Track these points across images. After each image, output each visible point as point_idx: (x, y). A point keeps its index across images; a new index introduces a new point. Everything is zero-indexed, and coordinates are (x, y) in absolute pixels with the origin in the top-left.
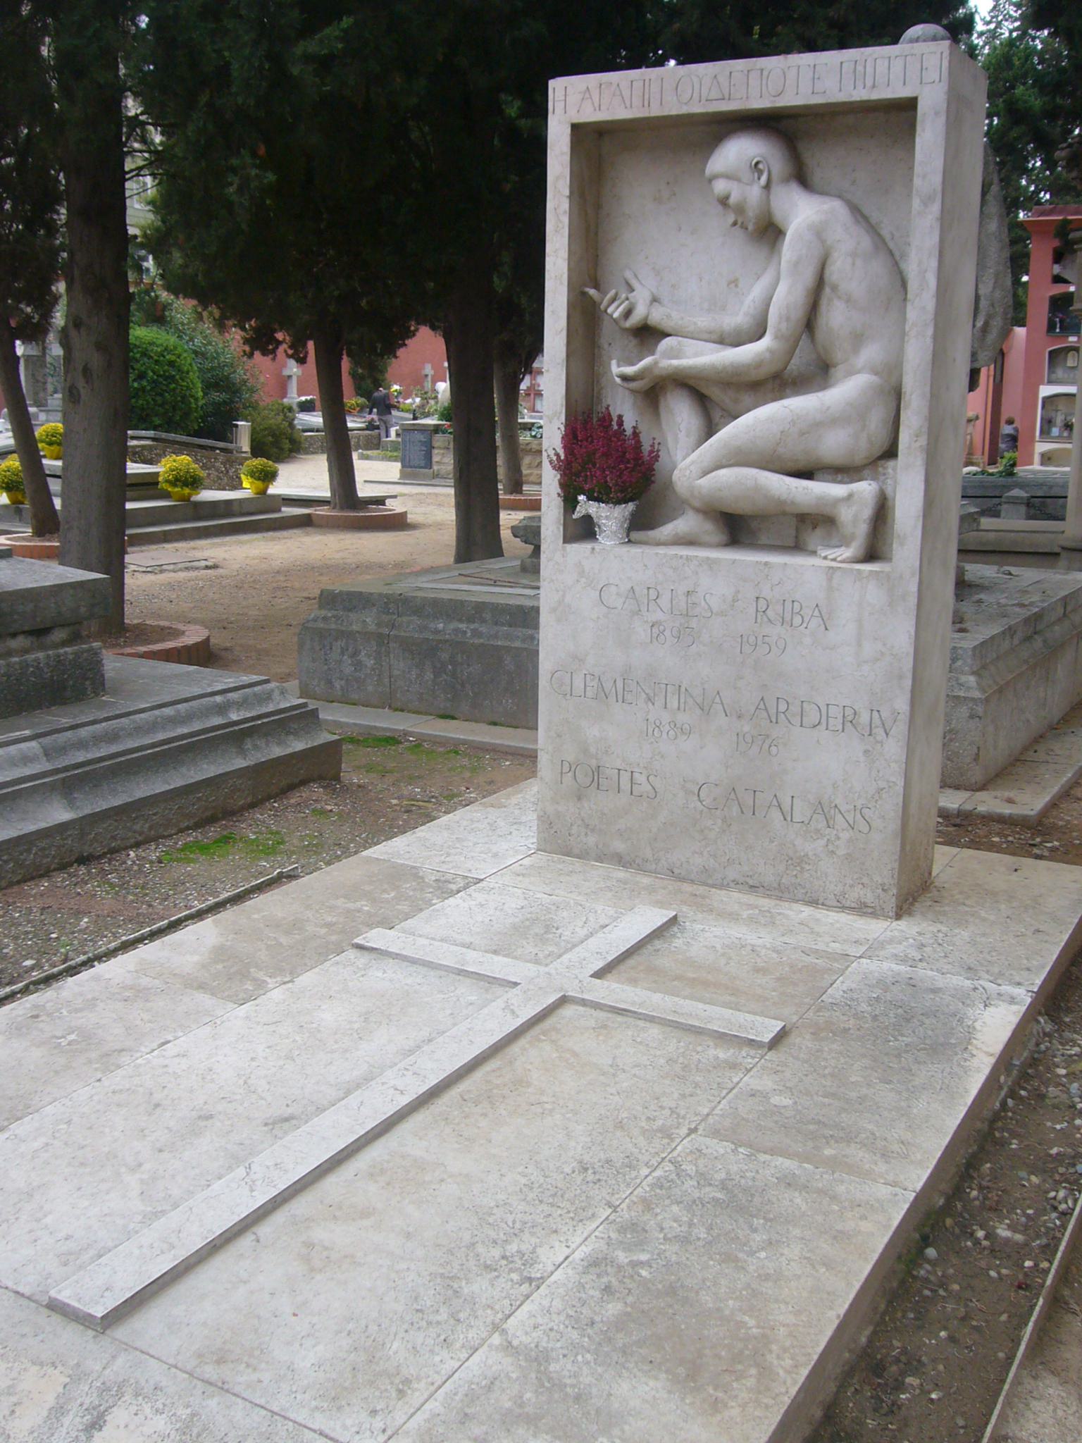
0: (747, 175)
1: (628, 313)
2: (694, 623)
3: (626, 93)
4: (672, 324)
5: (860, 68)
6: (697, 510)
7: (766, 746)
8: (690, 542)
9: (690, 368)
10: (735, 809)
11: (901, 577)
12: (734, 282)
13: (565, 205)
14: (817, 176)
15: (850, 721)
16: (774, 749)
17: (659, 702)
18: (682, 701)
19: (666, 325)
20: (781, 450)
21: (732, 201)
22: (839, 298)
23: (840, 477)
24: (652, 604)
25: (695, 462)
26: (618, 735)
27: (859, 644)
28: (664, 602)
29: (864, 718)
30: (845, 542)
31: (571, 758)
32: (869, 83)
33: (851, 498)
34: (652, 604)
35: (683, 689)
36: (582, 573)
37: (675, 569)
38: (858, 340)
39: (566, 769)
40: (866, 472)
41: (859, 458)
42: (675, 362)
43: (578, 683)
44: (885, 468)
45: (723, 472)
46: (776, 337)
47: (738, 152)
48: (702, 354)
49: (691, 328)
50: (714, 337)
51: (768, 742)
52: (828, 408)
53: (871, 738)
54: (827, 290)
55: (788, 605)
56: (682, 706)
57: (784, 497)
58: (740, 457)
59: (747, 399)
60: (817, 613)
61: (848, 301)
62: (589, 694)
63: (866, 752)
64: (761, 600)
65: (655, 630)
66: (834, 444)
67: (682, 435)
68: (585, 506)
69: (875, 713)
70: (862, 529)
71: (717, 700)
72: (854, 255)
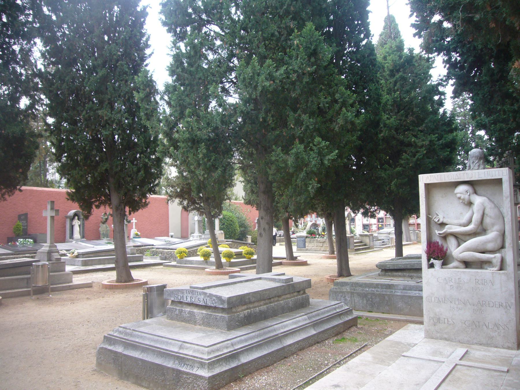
0: (465, 193)
1: (438, 221)
2: (461, 285)
6: (458, 261)
8: (457, 268)
10: (474, 327)
12: (462, 213)
13: (424, 199)
14: (479, 192)
15: (501, 305)
17: (453, 302)
19: (447, 222)
25: (457, 251)
28: (453, 281)
29: (504, 304)
31: (432, 316)
33: (496, 257)
38: (493, 225)
41: (496, 249)
42: (451, 230)
43: (433, 299)
46: (475, 225)
47: (462, 188)
54: (485, 215)
59: (468, 237)
66: (490, 246)
68: (432, 261)
70: (499, 264)
72: (491, 208)
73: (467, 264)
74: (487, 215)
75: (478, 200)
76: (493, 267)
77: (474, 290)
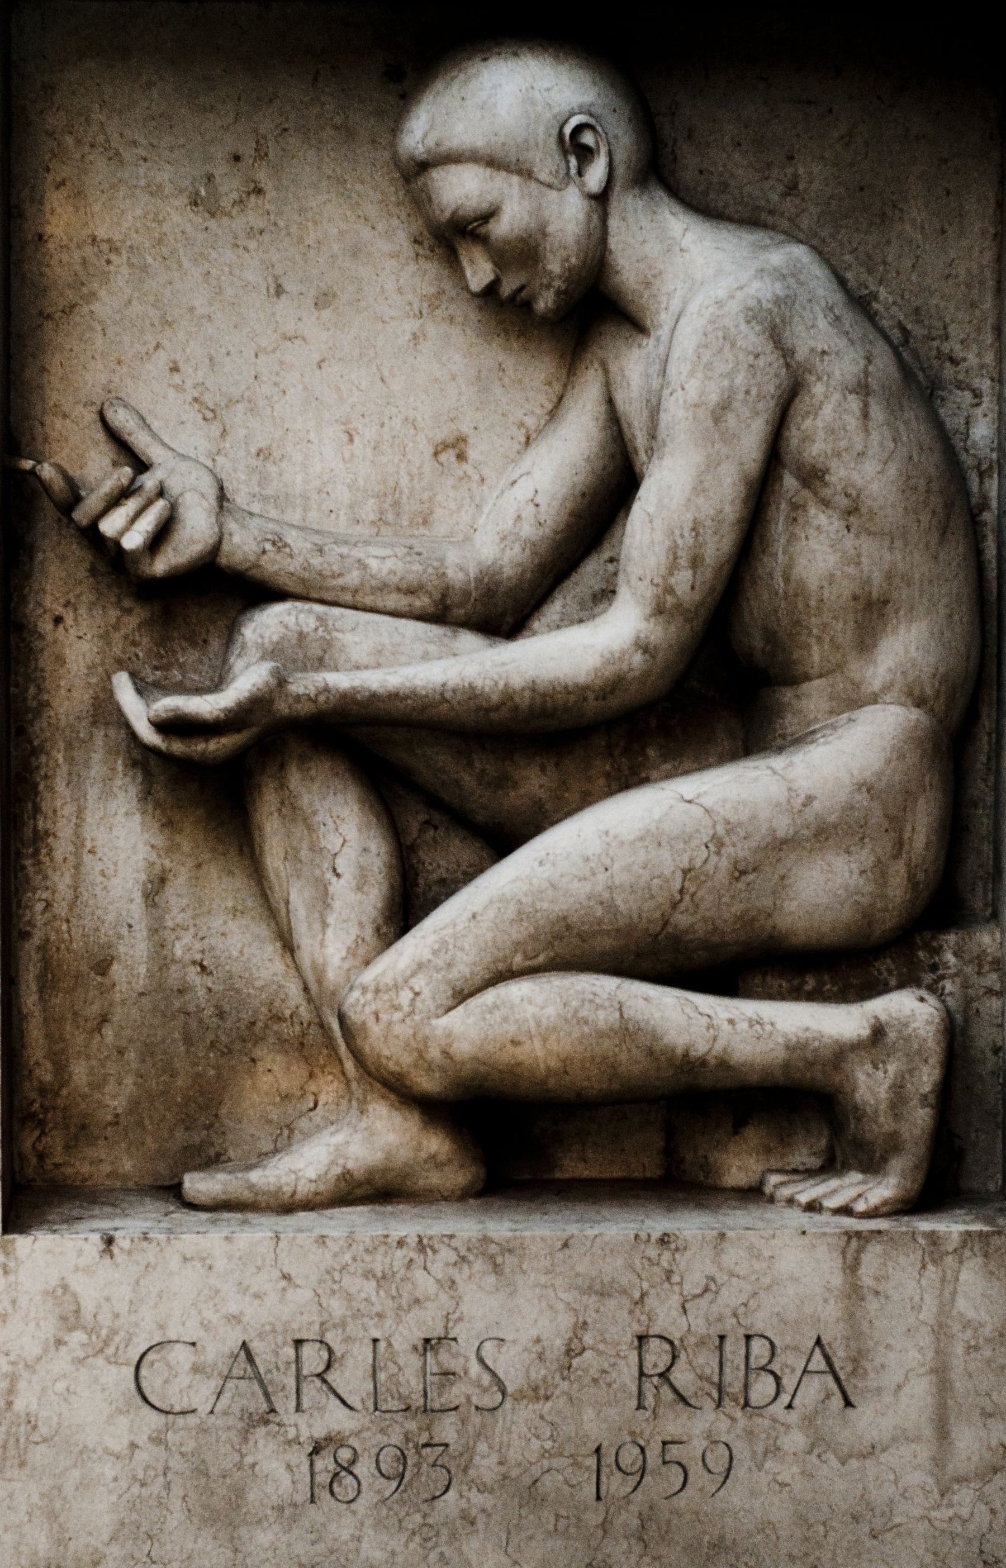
0: (547, 163)
1: (161, 535)
2: (447, 1430)
4: (294, 566)
9: (394, 696)
12: (456, 447)
14: (689, 164)
19: (275, 566)
20: (682, 920)
21: (502, 228)
22: (826, 503)
24: (312, 1390)
28: (352, 1379)
30: (872, 1165)
34: (312, 1390)
36: (72, 1319)
37: (383, 1279)
38: (872, 613)
40: (885, 966)
42: (341, 681)
44: (938, 951)
45: (517, 990)
49: (353, 578)
50: (421, 602)
52: (809, 799)
55: (734, 1349)
59: (534, 781)
60: (818, 1362)
64: (654, 1344)
65: (325, 1463)
66: (823, 893)
67: (341, 889)
72: (862, 389)
73: (511, 1138)
74: (813, 477)
76: (830, 1166)
77: (615, 1485)
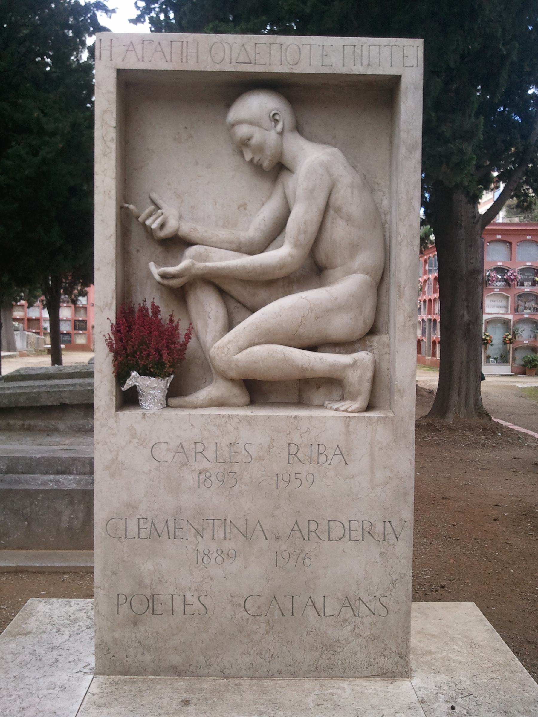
1: (162, 226)
2: (236, 468)
3: (167, 50)
4: (198, 235)
5: (358, 51)
6: (232, 380)
7: (301, 559)
8: (221, 404)
9: (224, 269)
10: (277, 613)
11: (402, 420)
12: (244, 206)
13: (113, 134)
15: (368, 532)
16: (307, 561)
17: (207, 535)
18: (228, 531)
19: (194, 235)
20: (301, 330)
21: (254, 141)
22: (341, 218)
23: (337, 350)
24: (199, 456)
25: (230, 343)
26: (171, 568)
27: (372, 473)
28: (210, 453)
29: (379, 528)
30: (353, 398)
31: (127, 590)
32: (365, 62)
33: (355, 364)
34: (199, 456)
35: (228, 522)
36: (134, 435)
37: (218, 426)
38: (354, 248)
39: (122, 599)
40: (358, 345)
41: (358, 334)
42: (209, 264)
43: (132, 526)
44: (372, 342)
45: (256, 348)
46: (296, 245)
47: (257, 106)
48: (226, 259)
49: (215, 239)
50: (234, 246)
51: (302, 556)
52: (336, 298)
53: (385, 543)
54: (331, 212)
55: (315, 447)
56: (228, 536)
57: (306, 365)
58: (269, 337)
59: (263, 294)
60: (338, 452)
61: (348, 221)
62: (143, 535)
63: (382, 554)
65: (202, 476)
66: (341, 325)
67: (211, 322)
68: (135, 379)
69: (388, 524)
70: (366, 386)
71: (258, 527)
73: (256, 389)
74: (338, 210)
75: (312, 158)
76: (343, 398)
77: (281, 484)
